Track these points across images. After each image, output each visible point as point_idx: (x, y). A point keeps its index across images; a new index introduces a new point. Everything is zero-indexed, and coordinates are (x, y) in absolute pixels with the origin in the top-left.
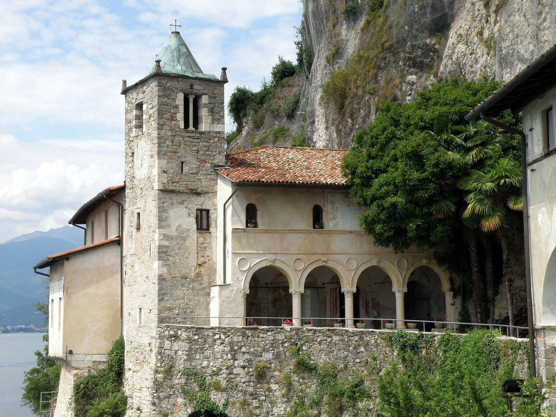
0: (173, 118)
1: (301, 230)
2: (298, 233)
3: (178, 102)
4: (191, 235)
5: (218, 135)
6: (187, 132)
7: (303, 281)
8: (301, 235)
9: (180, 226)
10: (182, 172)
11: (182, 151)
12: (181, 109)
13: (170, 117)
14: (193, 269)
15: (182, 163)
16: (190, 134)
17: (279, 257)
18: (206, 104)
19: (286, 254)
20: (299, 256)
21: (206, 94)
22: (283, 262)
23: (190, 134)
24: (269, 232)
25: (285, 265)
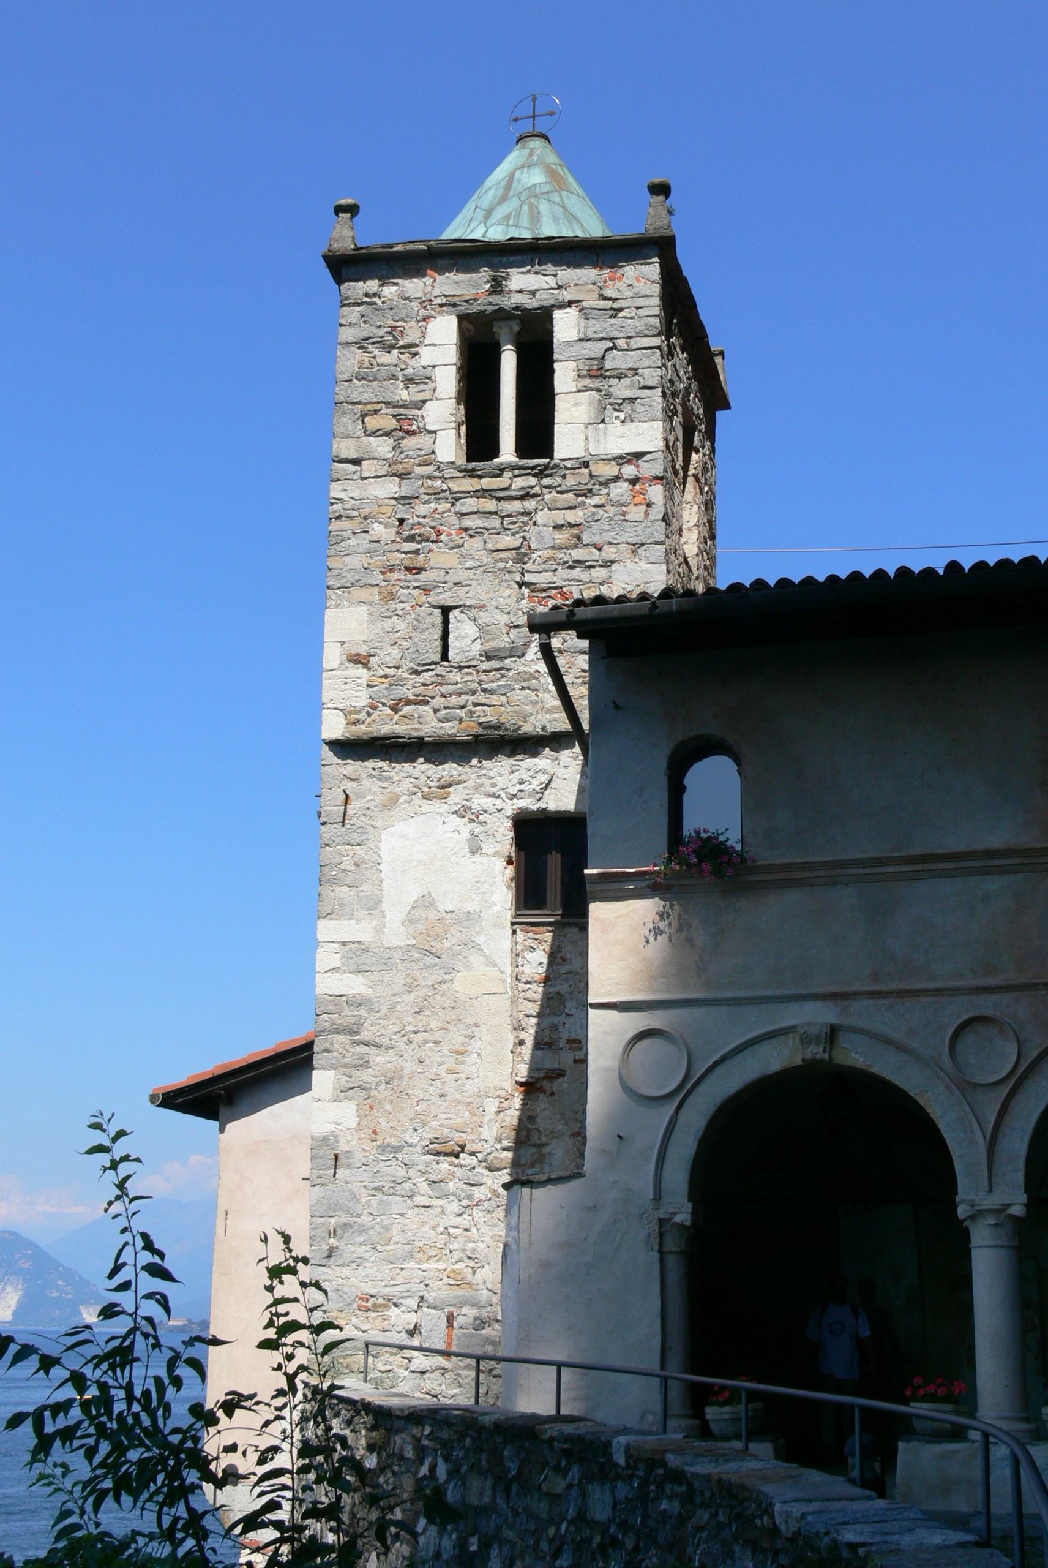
0: (405, 426)
1: (989, 854)
2: (969, 872)
3: (427, 356)
4: (480, 940)
5: (629, 471)
6: (471, 473)
7: (1017, 1144)
8: (994, 884)
9: (427, 901)
10: (445, 656)
11: (440, 558)
12: (447, 381)
13: (393, 424)
14: (492, 1105)
15: (446, 611)
16: (486, 483)
17: (862, 1014)
18: (568, 343)
19: (902, 994)
20: (986, 1005)
21: (570, 304)
22: (887, 1041)
23: (486, 483)
24: (798, 883)
25: (901, 1050)
